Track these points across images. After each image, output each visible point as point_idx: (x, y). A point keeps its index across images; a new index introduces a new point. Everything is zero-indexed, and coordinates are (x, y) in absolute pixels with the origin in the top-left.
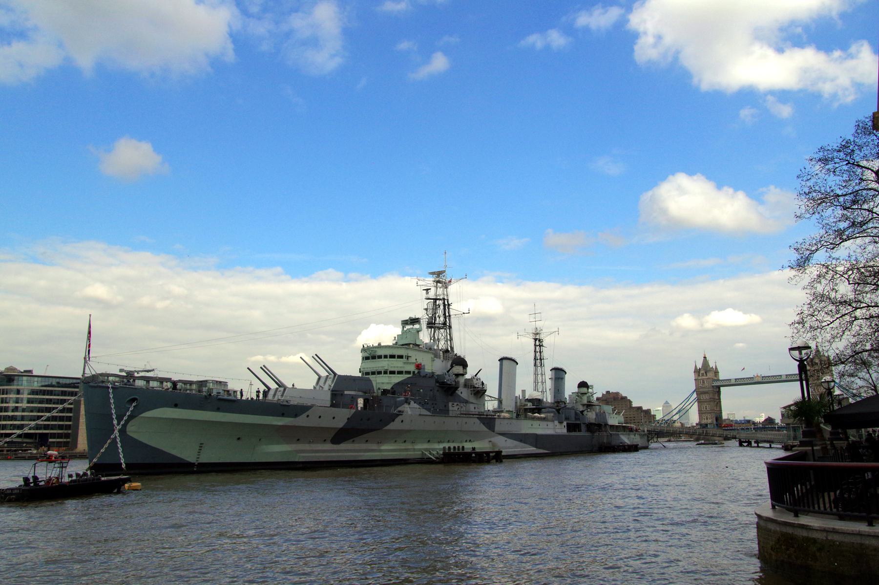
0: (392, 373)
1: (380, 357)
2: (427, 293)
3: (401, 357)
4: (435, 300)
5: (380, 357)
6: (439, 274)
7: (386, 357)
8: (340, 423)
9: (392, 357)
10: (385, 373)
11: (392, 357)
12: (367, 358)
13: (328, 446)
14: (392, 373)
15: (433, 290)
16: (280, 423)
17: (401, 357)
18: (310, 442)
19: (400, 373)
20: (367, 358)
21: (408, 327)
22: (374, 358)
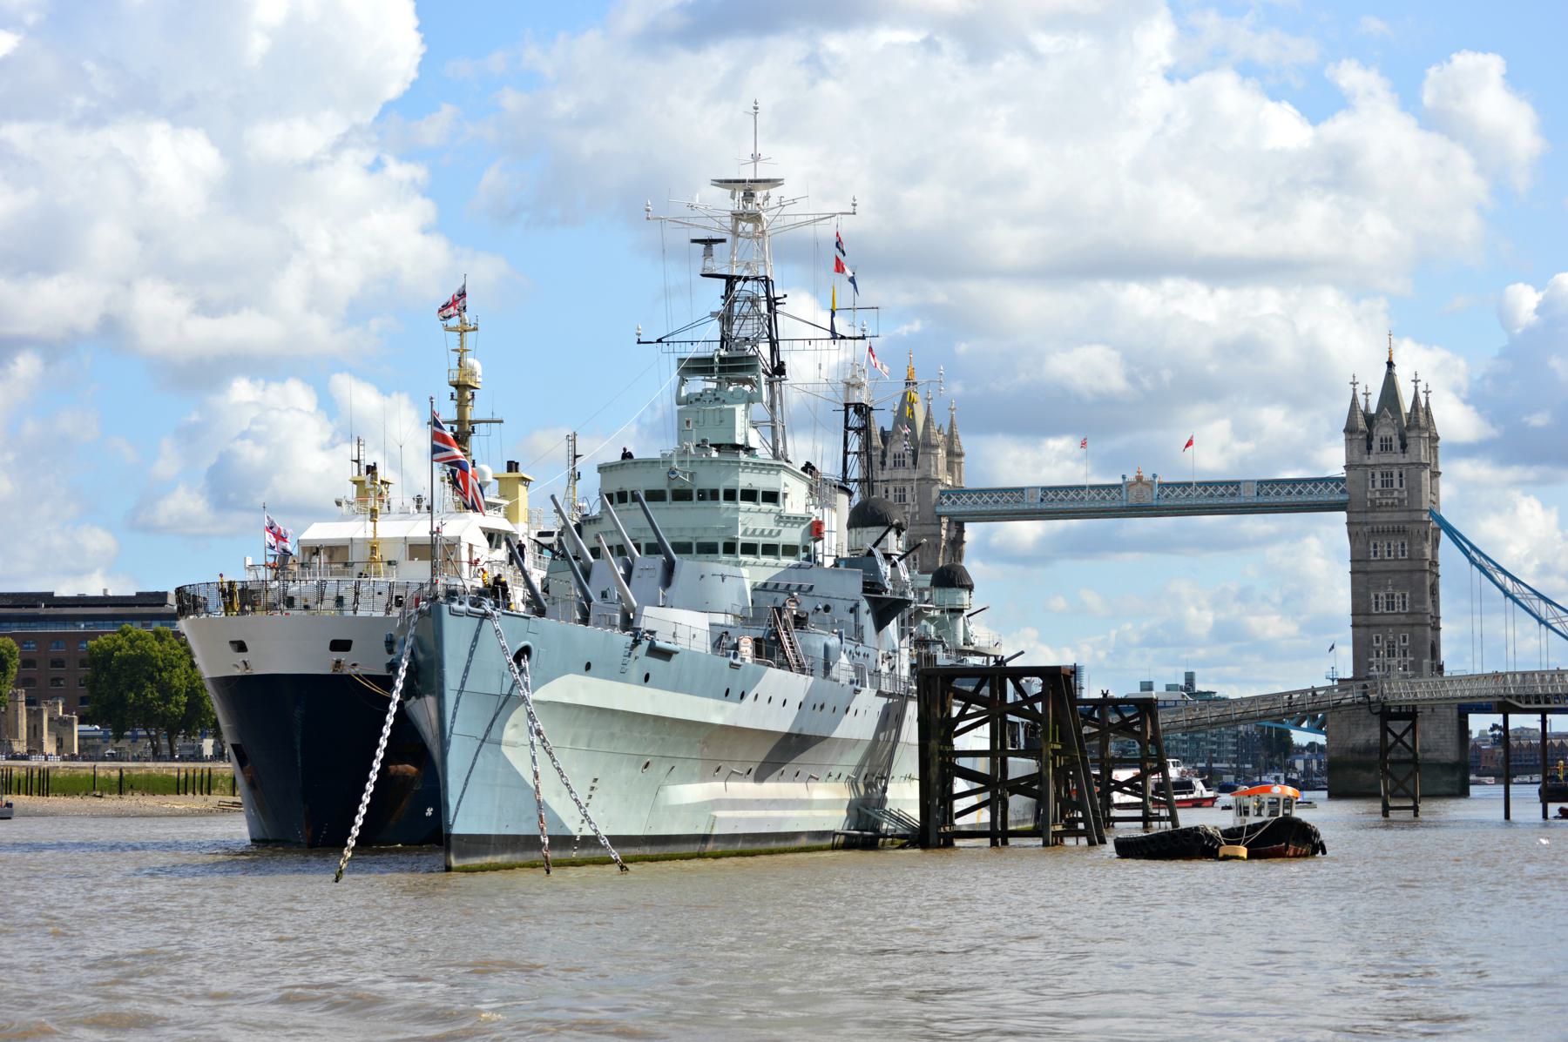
0: (749, 549)
2: (708, 254)
3: (771, 497)
4: (731, 280)
6: (748, 188)
7: (730, 495)
8: (782, 722)
9: (749, 495)
10: (730, 548)
11: (749, 495)
13: (747, 789)
14: (749, 549)
15: (729, 237)
16: (718, 719)
17: (771, 497)
18: (731, 776)
19: (770, 550)
21: (698, 384)
22: (682, 495)
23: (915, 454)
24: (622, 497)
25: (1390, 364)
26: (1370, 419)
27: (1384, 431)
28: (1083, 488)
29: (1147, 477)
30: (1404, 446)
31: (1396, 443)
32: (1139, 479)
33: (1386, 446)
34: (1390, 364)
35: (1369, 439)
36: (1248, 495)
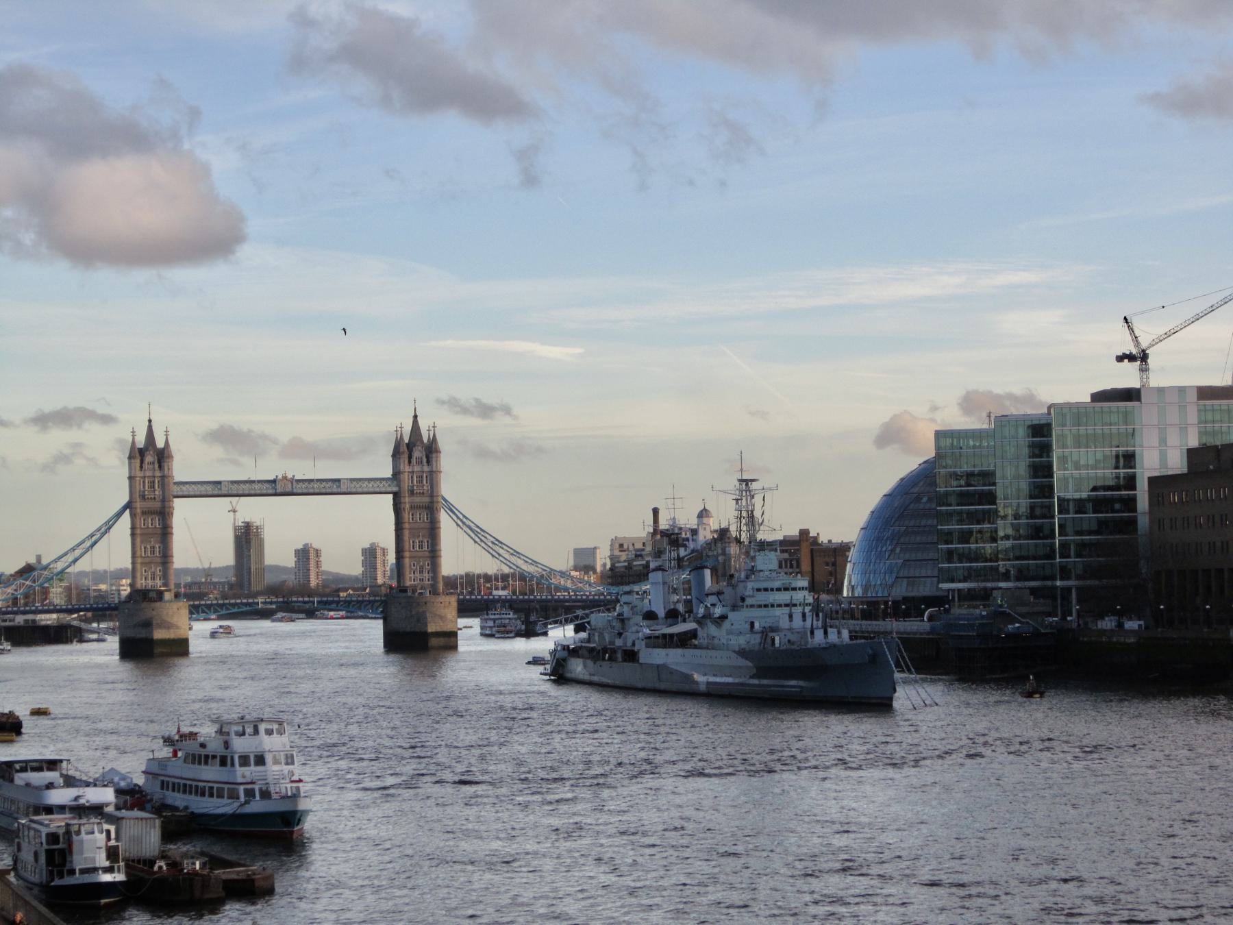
1: (794, 589)
5: (794, 589)
6: (747, 482)
12: (779, 590)
20: (779, 590)
22: (786, 589)
23: (159, 462)
24: (766, 590)
25: (415, 417)
26: (408, 445)
27: (417, 453)
28: (253, 482)
29: (290, 476)
30: (428, 462)
31: (425, 460)
32: (285, 478)
33: (420, 462)
34: (415, 417)
35: (410, 457)
36: (344, 489)
